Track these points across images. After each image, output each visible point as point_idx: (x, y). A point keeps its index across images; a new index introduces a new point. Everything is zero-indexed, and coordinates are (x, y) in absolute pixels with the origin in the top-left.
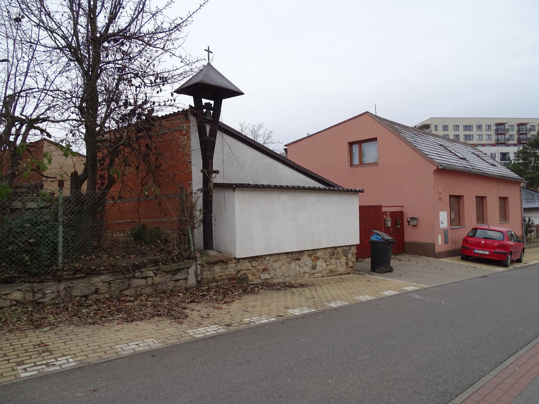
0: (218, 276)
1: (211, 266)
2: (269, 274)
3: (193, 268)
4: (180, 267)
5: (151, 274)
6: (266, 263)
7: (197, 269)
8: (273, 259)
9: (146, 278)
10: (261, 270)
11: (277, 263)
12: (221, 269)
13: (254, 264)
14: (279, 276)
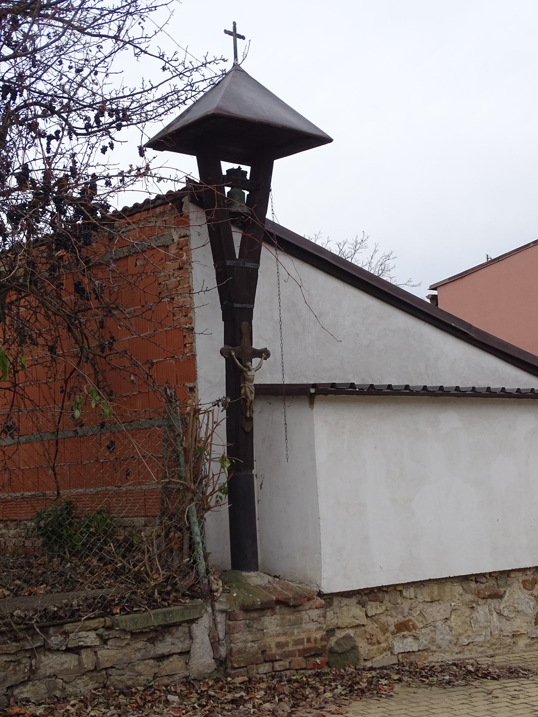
0: (273, 646)
1: (255, 615)
2: (416, 638)
3: (205, 621)
4: (171, 620)
5: (91, 638)
6: (406, 606)
7: (215, 625)
8: (424, 594)
9: (76, 650)
10: (392, 628)
11: (436, 607)
12: (282, 625)
13: (374, 609)
14: (444, 644)
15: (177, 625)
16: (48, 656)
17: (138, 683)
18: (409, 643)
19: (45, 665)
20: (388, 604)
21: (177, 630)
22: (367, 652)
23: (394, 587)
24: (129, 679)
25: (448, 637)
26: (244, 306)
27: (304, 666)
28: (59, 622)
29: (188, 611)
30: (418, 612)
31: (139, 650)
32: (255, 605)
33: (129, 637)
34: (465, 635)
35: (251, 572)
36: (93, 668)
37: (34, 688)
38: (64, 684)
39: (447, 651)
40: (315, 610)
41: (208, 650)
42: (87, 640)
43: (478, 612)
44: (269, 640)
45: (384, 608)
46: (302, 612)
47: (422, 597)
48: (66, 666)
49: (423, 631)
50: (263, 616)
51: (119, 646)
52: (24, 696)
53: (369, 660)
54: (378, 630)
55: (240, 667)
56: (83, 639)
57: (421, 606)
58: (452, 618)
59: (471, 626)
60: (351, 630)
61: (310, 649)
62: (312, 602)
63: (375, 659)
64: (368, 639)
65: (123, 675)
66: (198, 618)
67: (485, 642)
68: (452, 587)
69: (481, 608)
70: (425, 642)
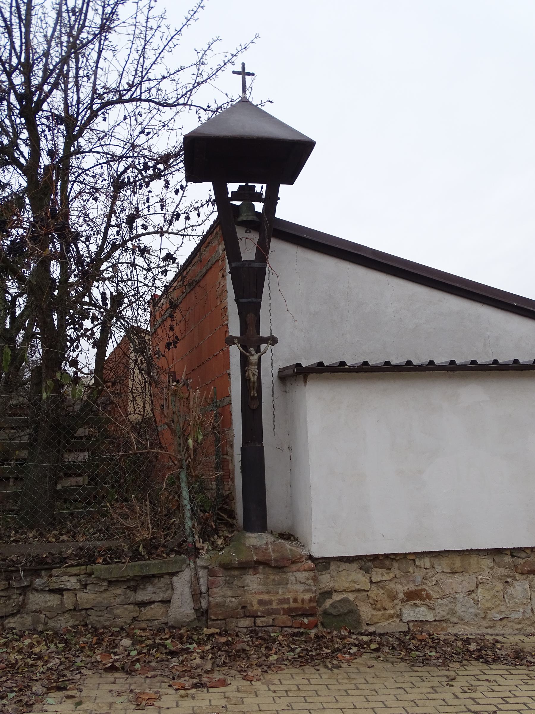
0: (255, 602)
1: (236, 573)
2: (430, 608)
3: (186, 575)
4: (145, 572)
5: (72, 582)
6: (419, 575)
7: (198, 580)
8: (443, 565)
9: (60, 591)
10: (401, 596)
11: (458, 578)
12: (265, 584)
13: (378, 575)
14: (467, 617)
15: (161, 576)
16: (34, 594)
17: (116, 624)
18: (421, 612)
19: (32, 602)
20: (398, 572)
21: (159, 581)
22: (370, 617)
23: (405, 555)
24: (105, 621)
25: (472, 610)
26: (250, 300)
27: (289, 624)
28: (48, 566)
29: (167, 565)
30: (434, 582)
31: (119, 595)
32: (231, 564)
33: (106, 584)
34: (497, 610)
35: (255, 533)
36: (73, 608)
37: (22, 620)
38: (47, 619)
39: (472, 624)
40: (303, 572)
41: (188, 601)
42: (68, 584)
43: (514, 587)
44: (250, 596)
45: (392, 575)
46: (289, 573)
47: (440, 568)
48: (49, 604)
49: (440, 601)
50: (245, 574)
51: (98, 591)
52: (11, 625)
53: (372, 625)
54: (385, 596)
55: (218, 620)
56: (65, 583)
57: (439, 577)
58: (479, 591)
59: (505, 601)
60: (350, 594)
61: (295, 609)
62: (299, 565)
63: (379, 625)
64: (372, 604)
65: (101, 616)
66: (177, 573)
67: (523, 619)
68: (480, 560)
69: (518, 584)
70: (442, 613)
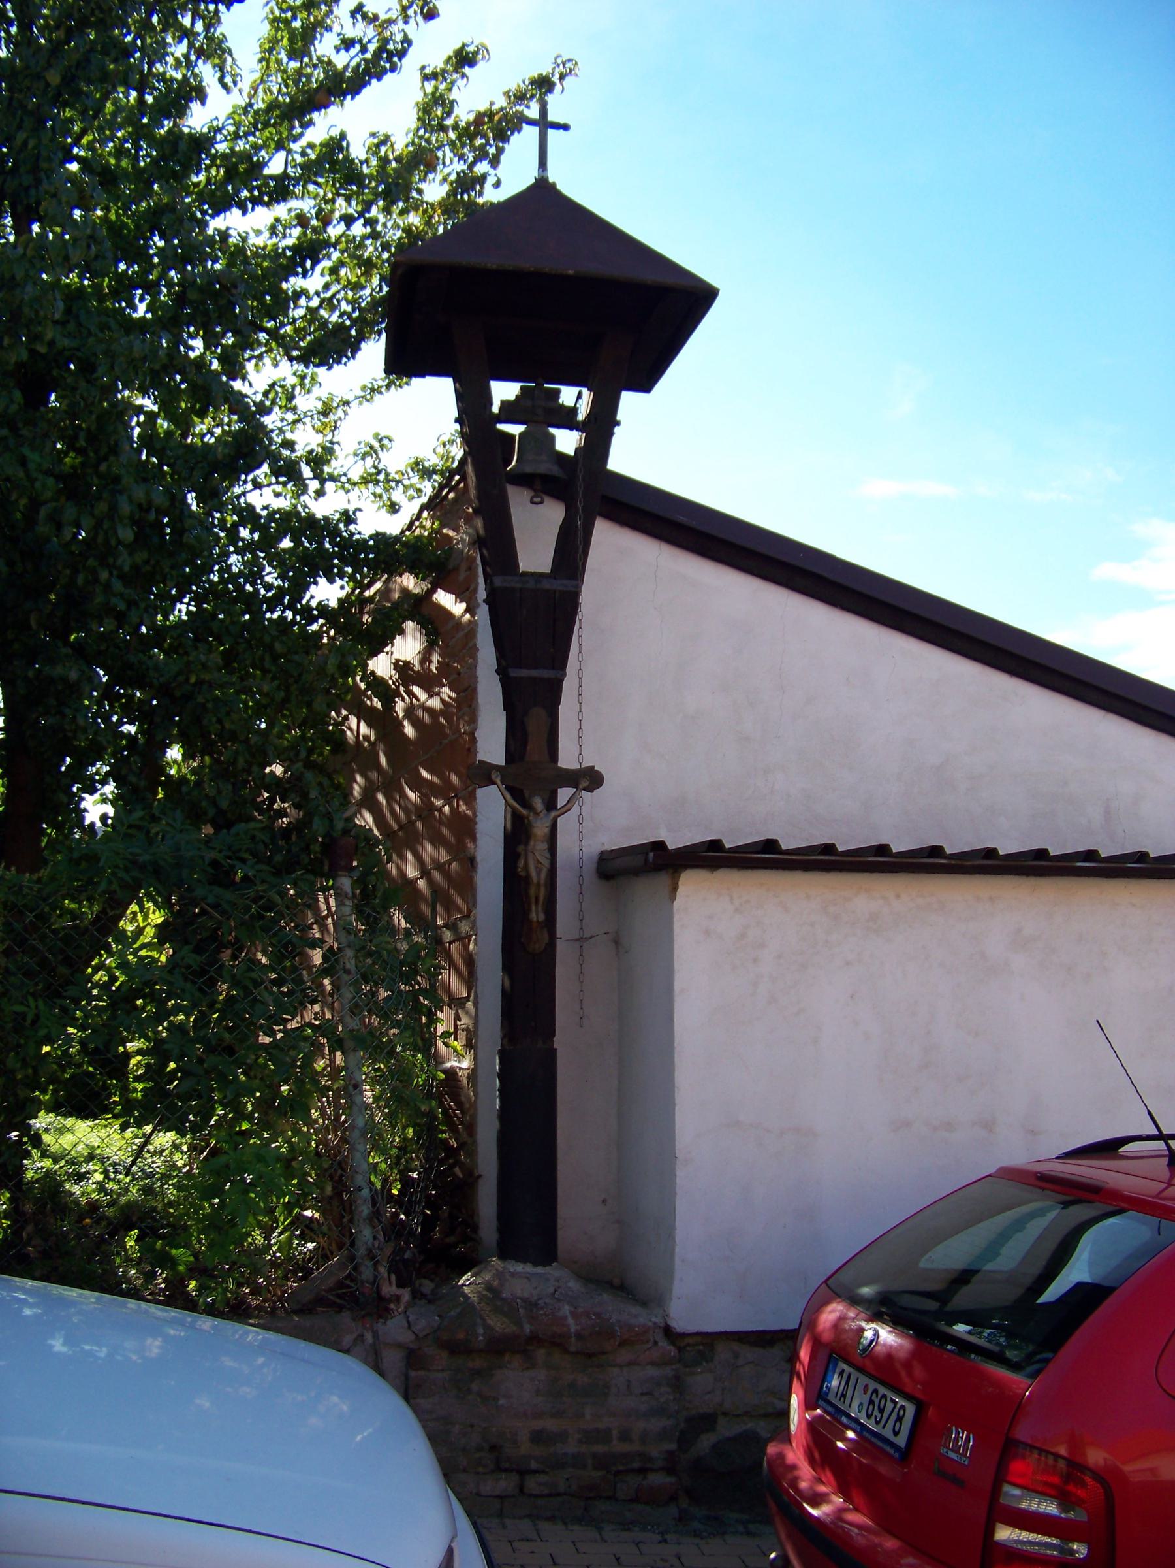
1: (478, 1363)
